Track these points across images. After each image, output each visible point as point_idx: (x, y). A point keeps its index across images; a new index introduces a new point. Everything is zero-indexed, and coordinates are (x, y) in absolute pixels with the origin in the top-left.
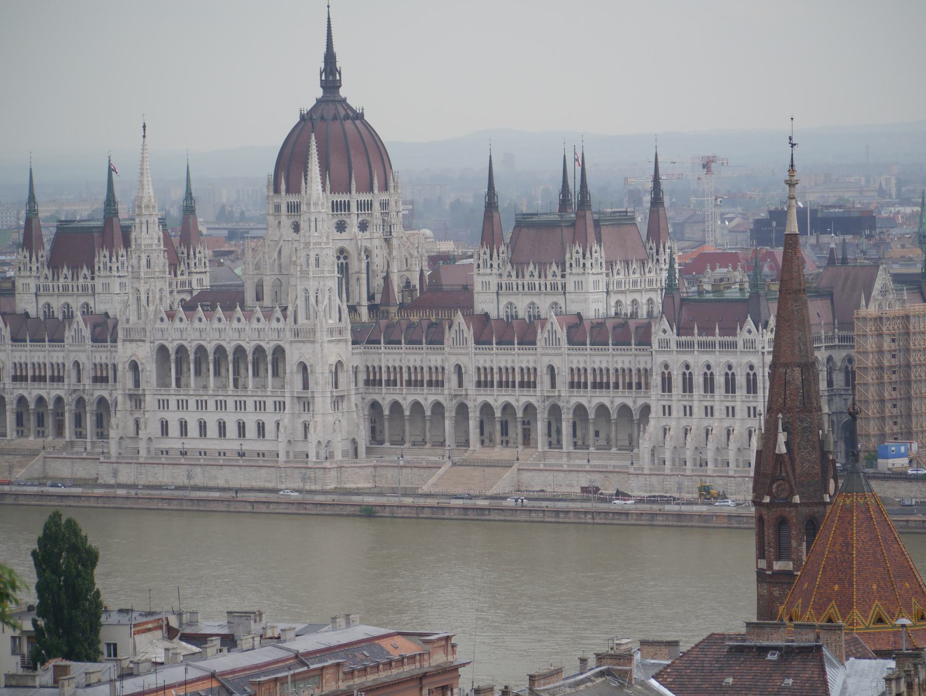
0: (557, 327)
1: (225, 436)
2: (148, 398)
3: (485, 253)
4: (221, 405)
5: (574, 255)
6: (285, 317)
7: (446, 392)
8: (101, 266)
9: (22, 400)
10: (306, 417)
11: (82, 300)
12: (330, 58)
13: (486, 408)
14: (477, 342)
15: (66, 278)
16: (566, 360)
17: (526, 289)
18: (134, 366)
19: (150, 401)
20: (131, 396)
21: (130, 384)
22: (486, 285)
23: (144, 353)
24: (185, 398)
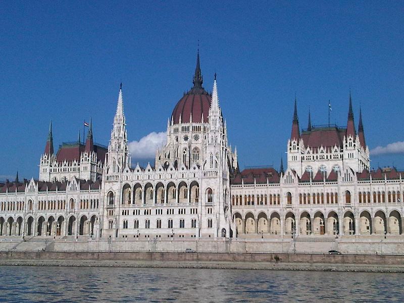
0: (350, 171)
1: (160, 227)
3: (294, 143)
4: (159, 212)
6: (199, 167)
7: (281, 206)
8: (84, 159)
9: (41, 219)
12: (198, 71)
16: (357, 188)
17: (319, 159)
18: (111, 195)
19: (118, 210)
22: (295, 158)
23: (116, 188)
24: (138, 209)
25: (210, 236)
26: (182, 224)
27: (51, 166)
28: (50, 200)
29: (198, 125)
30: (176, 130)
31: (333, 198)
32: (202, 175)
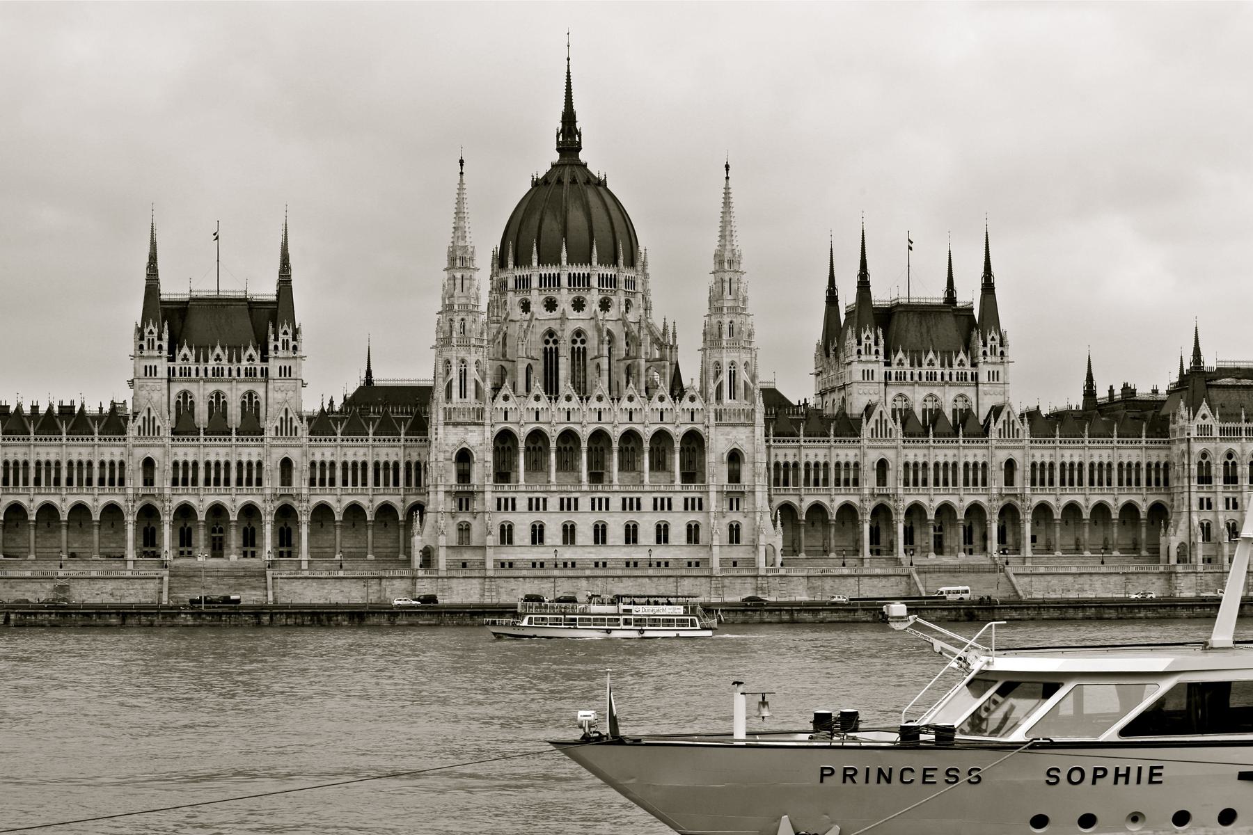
1: (604, 541)
2: (488, 496)
3: (868, 338)
4: (600, 505)
5: (989, 343)
8: (280, 344)
9: (185, 512)
10: (735, 517)
11: (245, 387)
12: (569, 118)
13: (915, 511)
14: (905, 435)
15: (218, 358)
16: (1029, 453)
17: (924, 379)
18: (464, 457)
20: (457, 492)
21: (453, 479)
22: (868, 375)
23: (480, 441)
25: (735, 564)
26: (662, 534)
27: (172, 359)
28: (213, 459)
29: (610, 271)
30: (554, 281)
31: (977, 474)
32: (712, 415)
